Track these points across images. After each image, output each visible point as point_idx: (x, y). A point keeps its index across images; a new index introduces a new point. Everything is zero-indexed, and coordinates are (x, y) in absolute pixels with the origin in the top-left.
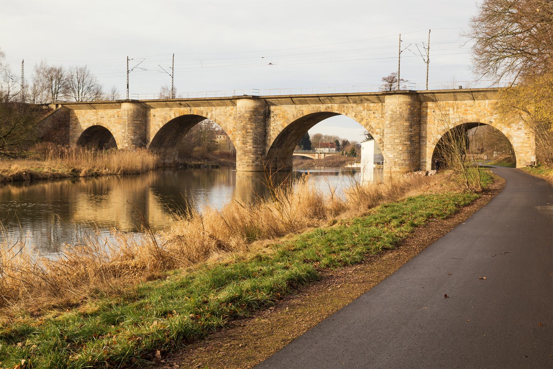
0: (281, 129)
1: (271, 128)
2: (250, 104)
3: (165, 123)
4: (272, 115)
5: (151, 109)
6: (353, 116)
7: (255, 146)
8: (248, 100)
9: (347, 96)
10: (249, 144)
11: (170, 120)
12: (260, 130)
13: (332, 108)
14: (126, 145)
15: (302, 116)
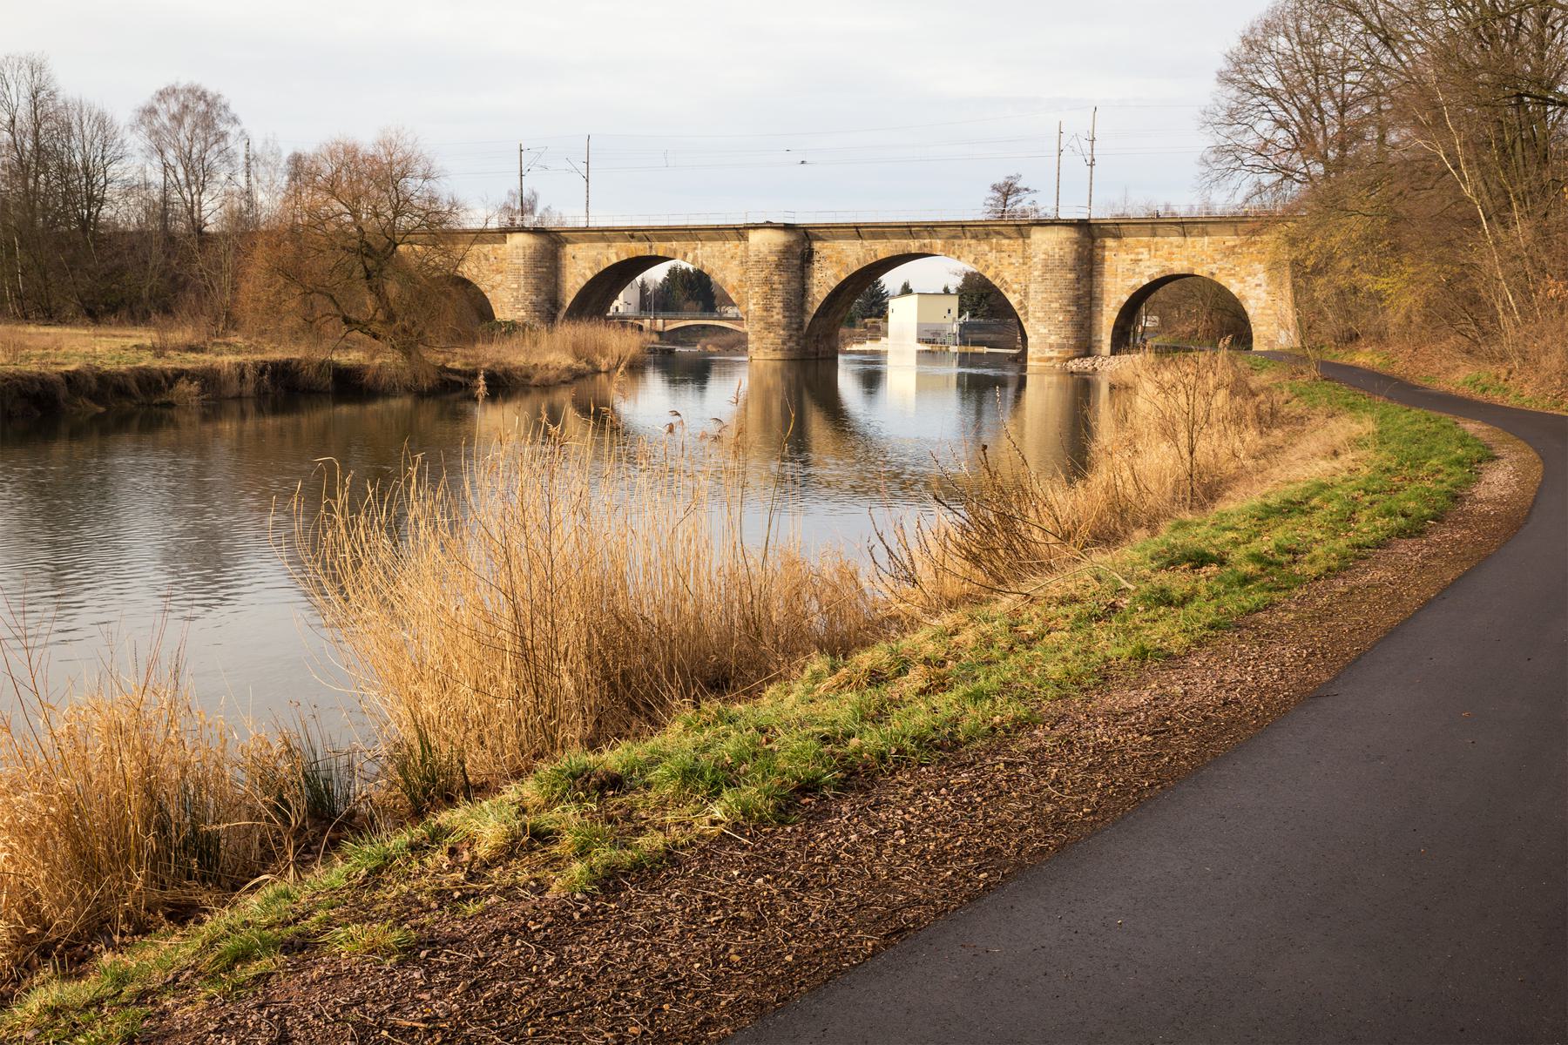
0: (833, 284)
1: (815, 281)
2: (779, 238)
3: (596, 272)
4: (816, 257)
5: (568, 246)
6: (972, 260)
7: (787, 314)
8: (775, 231)
9: (963, 226)
10: (776, 311)
11: (607, 265)
12: (795, 285)
13: (931, 246)
14: (522, 313)
15: (874, 260)
